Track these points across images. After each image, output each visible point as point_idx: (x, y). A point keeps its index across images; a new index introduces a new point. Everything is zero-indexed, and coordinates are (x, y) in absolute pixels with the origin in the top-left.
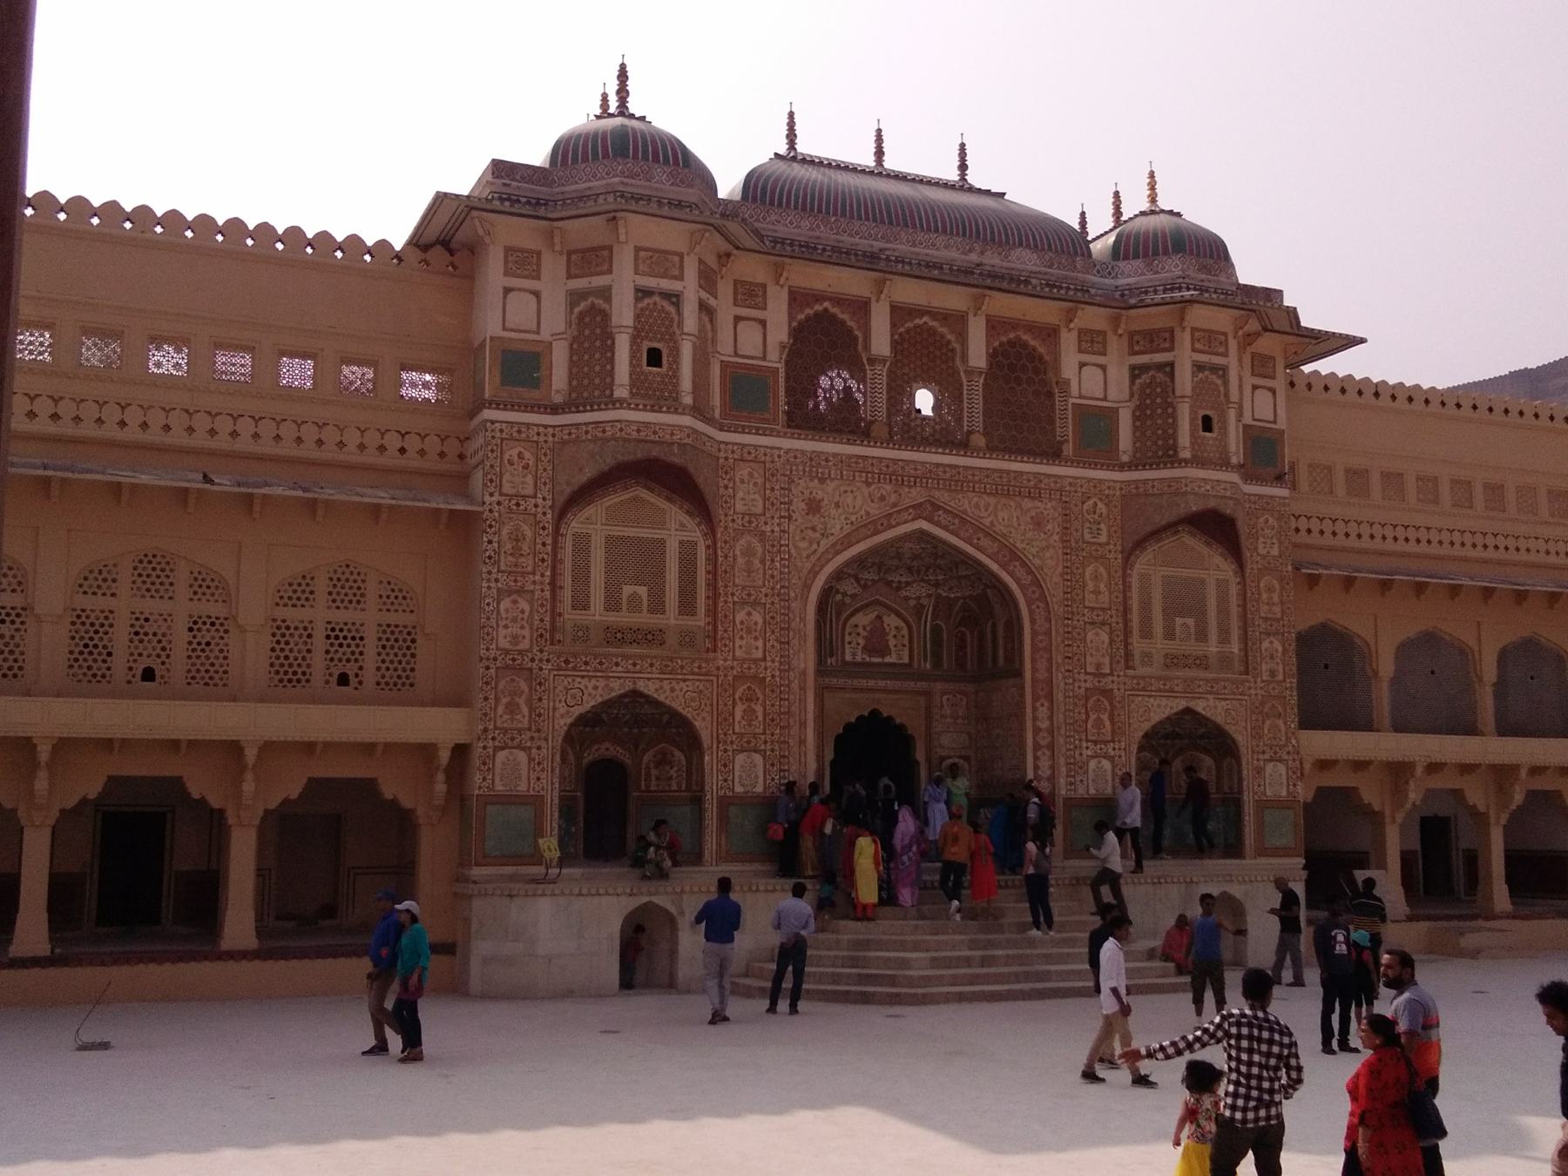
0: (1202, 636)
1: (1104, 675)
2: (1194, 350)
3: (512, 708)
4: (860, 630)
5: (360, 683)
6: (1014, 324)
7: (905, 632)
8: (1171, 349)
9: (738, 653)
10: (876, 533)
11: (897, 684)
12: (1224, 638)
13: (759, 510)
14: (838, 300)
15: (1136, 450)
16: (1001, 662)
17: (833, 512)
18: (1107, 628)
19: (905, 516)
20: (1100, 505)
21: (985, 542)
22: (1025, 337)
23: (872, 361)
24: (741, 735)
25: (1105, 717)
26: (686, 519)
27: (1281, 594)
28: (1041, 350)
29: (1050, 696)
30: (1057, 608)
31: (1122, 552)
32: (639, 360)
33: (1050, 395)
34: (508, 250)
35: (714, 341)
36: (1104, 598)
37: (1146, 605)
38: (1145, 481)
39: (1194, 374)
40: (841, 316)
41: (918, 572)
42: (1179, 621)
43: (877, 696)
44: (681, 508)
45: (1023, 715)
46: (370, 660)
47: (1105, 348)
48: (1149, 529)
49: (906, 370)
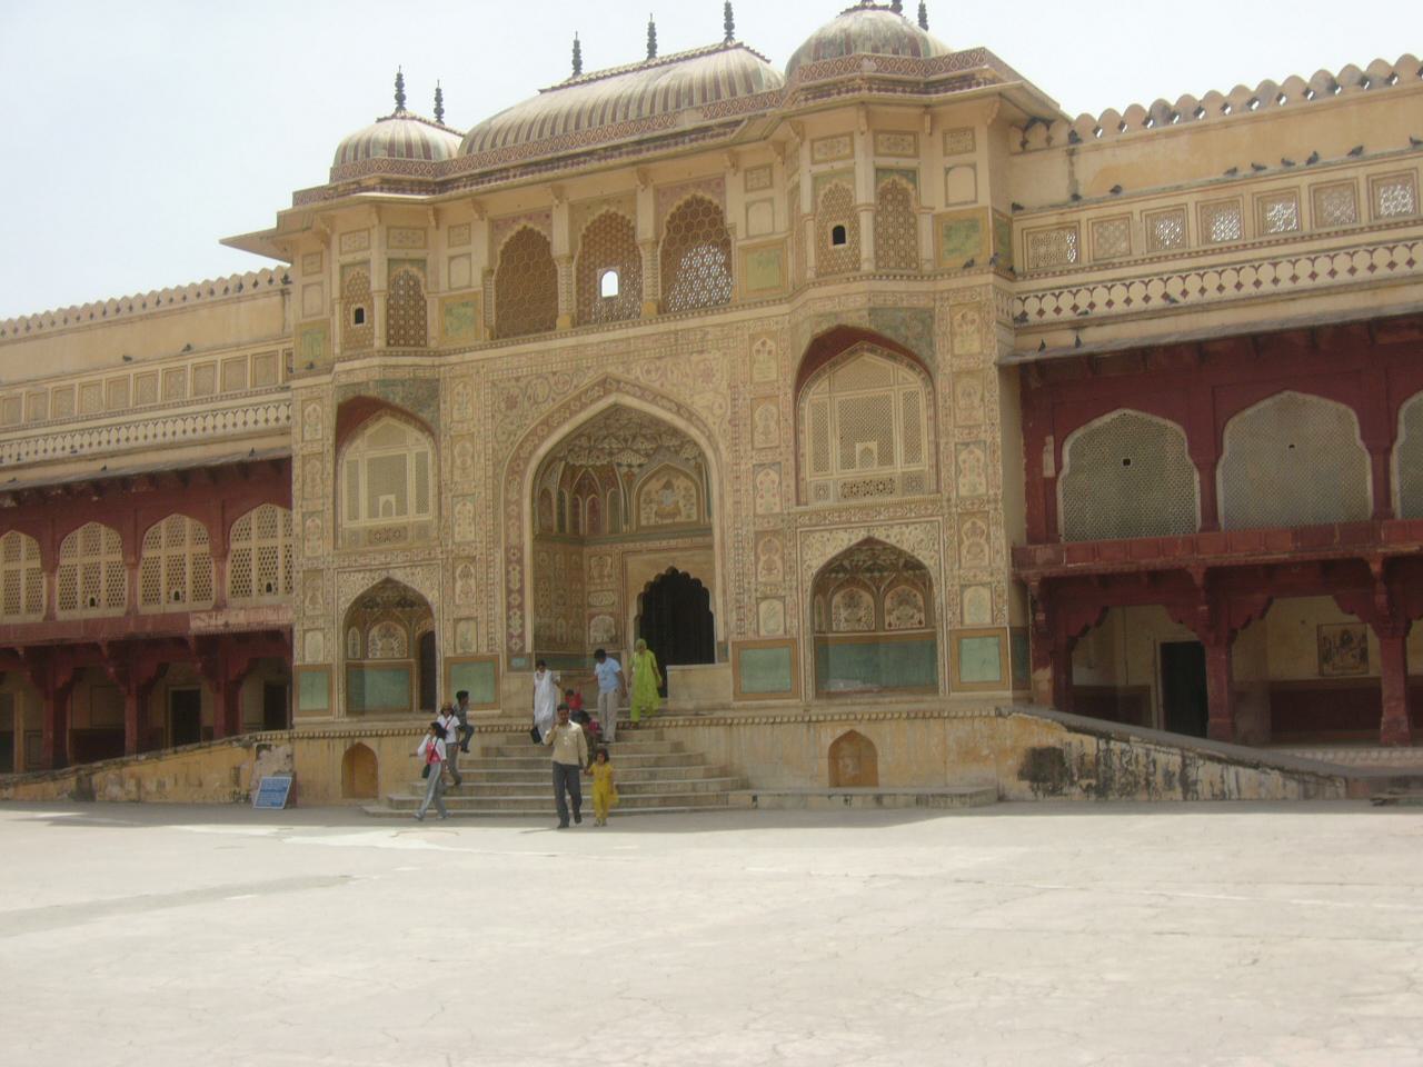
0: (886, 457)
2: (814, 162)
3: (313, 600)
4: (654, 496)
5: (277, 589)
6: (684, 187)
7: (693, 491)
8: (797, 170)
9: (458, 538)
10: (573, 413)
11: (687, 542)
12: (913, 451)
14: (530, 217)
18: (777, 467)
20: (770, 343)
21: (665, 402)
22: (700, 194)
25: (776, 558)
27: (982, 400)
28: (716, 201)
30: (726, 456)
32: (348, 320)
34: (304, 257)
35: (426, 287)
37: (820, 437)
39: (815, 189)
40: (537, 229)
42: (859, 447)
43: (674, 554)
46: (281, 573)
47: (771, 183)
49: (592, 259)
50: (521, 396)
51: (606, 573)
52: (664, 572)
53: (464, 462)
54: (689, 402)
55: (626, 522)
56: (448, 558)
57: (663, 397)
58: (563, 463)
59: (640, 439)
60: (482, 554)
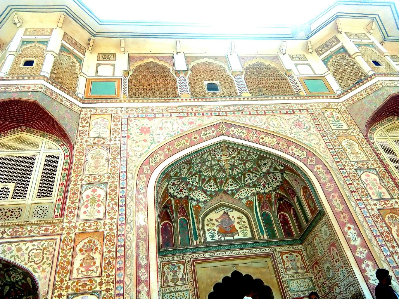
1: (388, 199)
4: (214, 222)
7: (245, 219)
9: (82, 217)
10: (193, 144)
11: (248, 251)
13: (108, 134)
15: (343, 88)
16: (309, 215)
17: (158, 131)
19: (210, 133)
20: (334, 114)
21: (267, 139)
23: (177, 73)
24: (78, 280)
26: (51, 143)
29: (352, 221)
31: (361, 131)
33: (284, 79)
36: (362, 157)
38: (355, 95)
41: (240, 179)
44: (50, 139)
45: (338, 240)
48: (370, 114)
50: (153, 127)
51: (179, 277)
52: (229, 275)
53: (97, 162)
54: (291, 136)
55: (196, 240)
56: (68, 234)
57: (267, 134)
58: (167, 183)
59: (212, 182)
60: (111, 229)
